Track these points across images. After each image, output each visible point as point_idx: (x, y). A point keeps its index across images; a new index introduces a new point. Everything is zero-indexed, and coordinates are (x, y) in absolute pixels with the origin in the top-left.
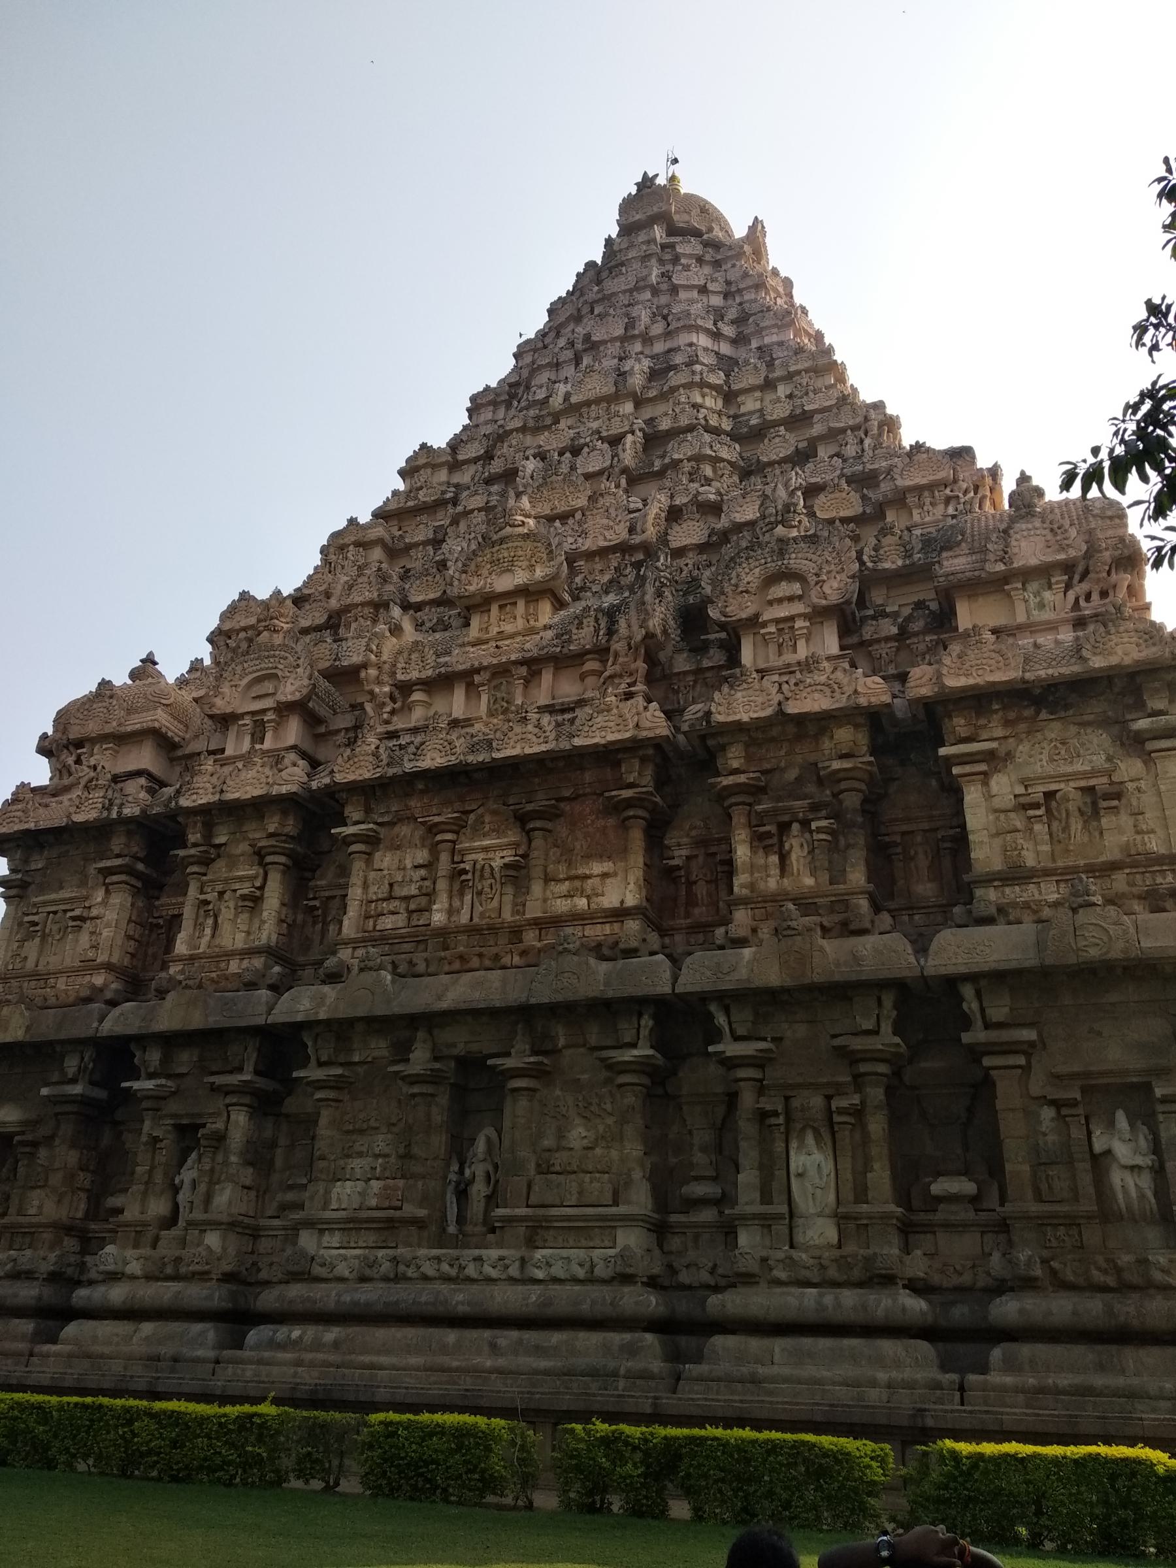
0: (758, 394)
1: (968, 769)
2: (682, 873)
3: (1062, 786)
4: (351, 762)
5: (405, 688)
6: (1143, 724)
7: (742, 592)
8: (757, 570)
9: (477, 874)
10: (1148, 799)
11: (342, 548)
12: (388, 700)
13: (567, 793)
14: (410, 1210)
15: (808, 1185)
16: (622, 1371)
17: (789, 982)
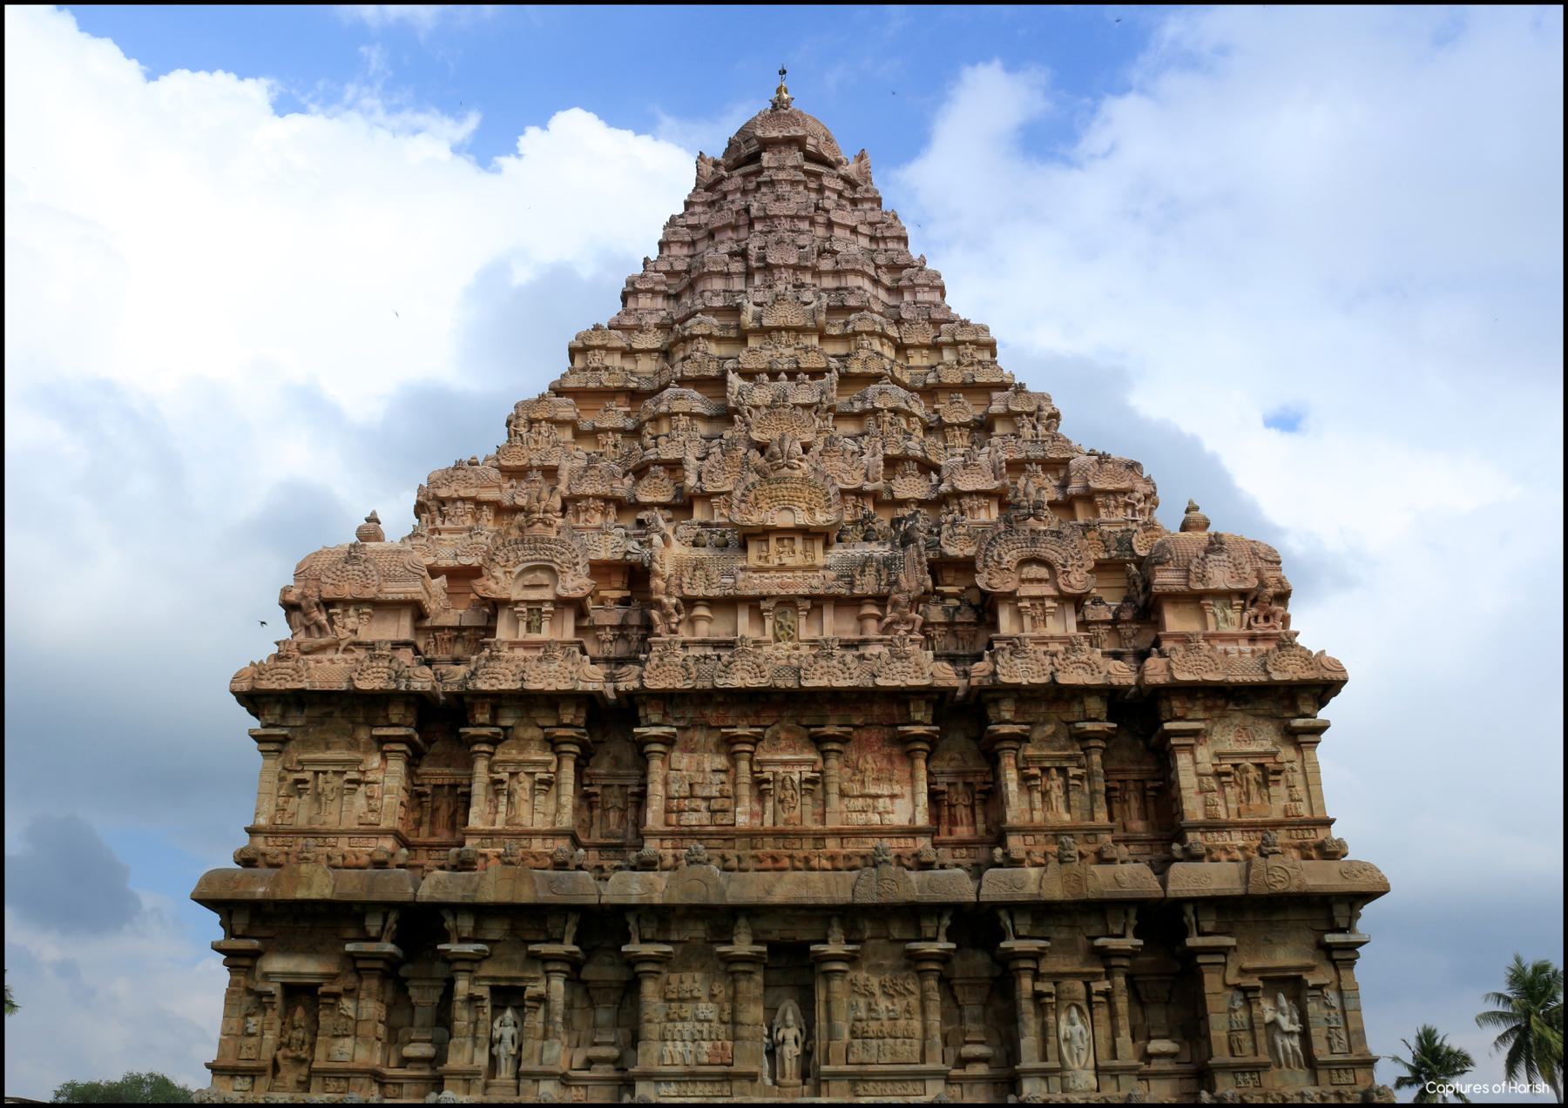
0: (925, 352)
1: (1182, 741)
2: (946, 797)
3: (1243, 761)
5: (689, 603)
6: (1299, 722)
8: (1015, 552)
10: (1298, 777)
11: (531, 422)
12: (673, 611)
13: (857, 722)
15: (1074, 1047)
17: (1070, 898)
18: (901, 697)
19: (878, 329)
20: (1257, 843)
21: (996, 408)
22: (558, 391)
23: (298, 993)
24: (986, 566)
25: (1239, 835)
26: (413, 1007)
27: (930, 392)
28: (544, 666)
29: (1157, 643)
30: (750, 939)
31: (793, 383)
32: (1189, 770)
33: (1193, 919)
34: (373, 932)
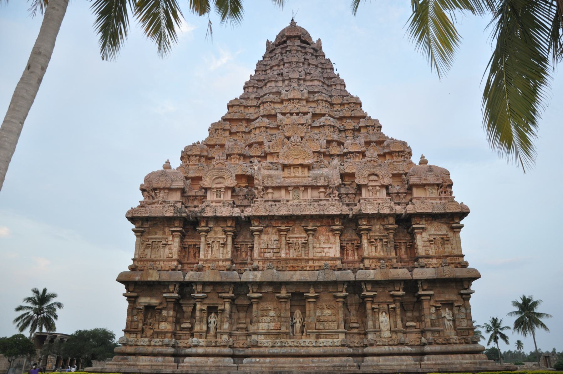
0: (339, 106)
1: (418, 231)
5: (267, 188)
6: (454, 225)
9: (294, 244)
11: (216, 130)
14: (284, 329)
16: (347, 365)
17: (383, 279)
18: (333, 217)
19: (324, 99)
20: (441, 262)
21: (361, 124)
22: (224, 119)
23: (149, 308)
25: (435, 260)
26: (184, 312)
27: (341, 119)
28: (222, 209)
29: (411, 200)
30: (286, 292)
31: (297, 117)
32: (420, 240)
33: (421, 286)
34: (171, 290)
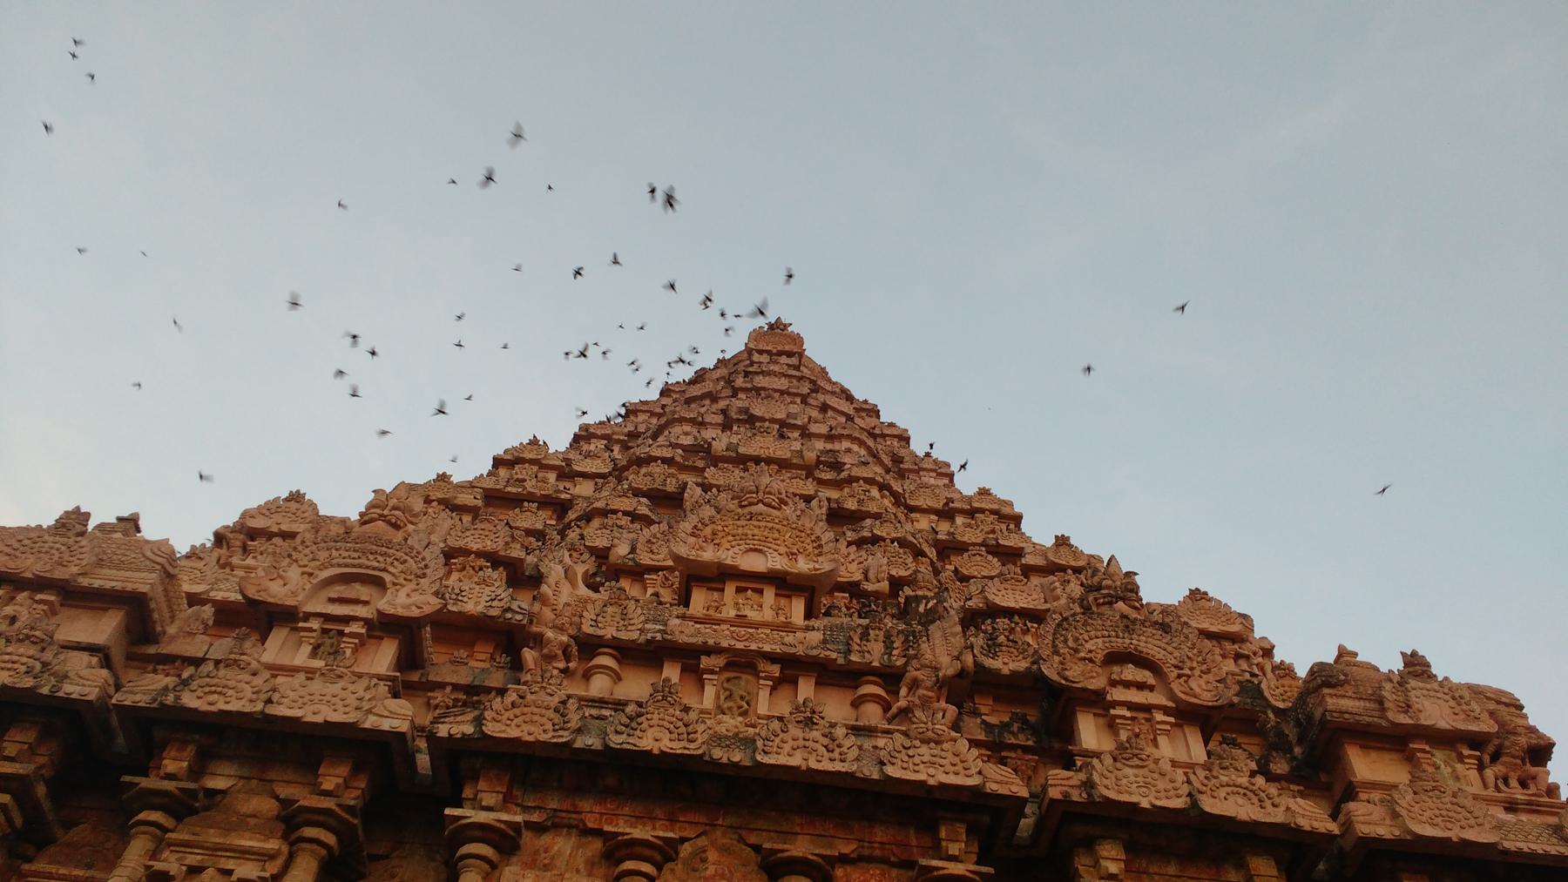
4: (517, 711)
5: (588, 646)
7: (1084, 659)
12: (560, 652)
24: (1056, 652)
